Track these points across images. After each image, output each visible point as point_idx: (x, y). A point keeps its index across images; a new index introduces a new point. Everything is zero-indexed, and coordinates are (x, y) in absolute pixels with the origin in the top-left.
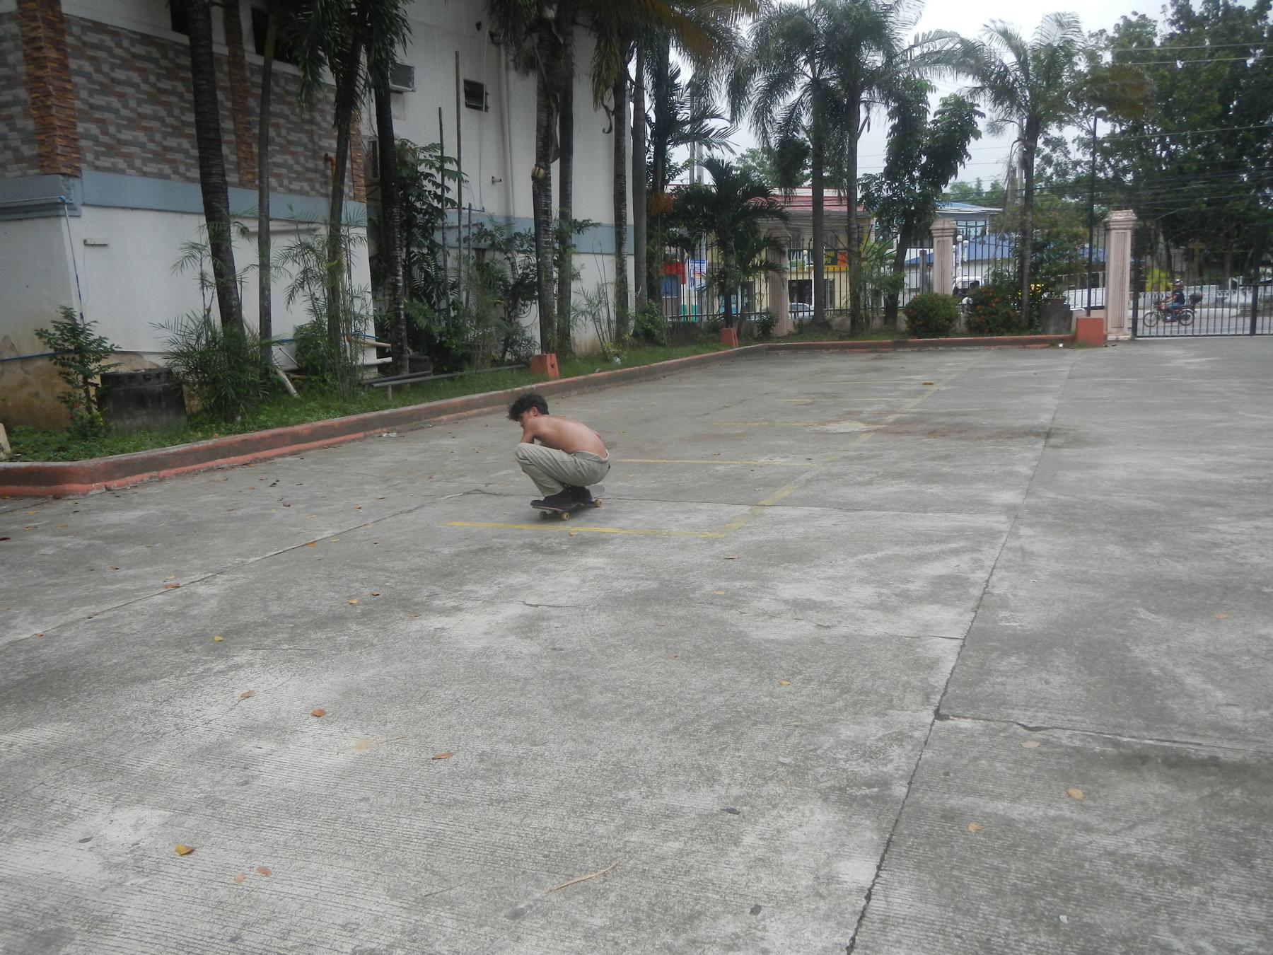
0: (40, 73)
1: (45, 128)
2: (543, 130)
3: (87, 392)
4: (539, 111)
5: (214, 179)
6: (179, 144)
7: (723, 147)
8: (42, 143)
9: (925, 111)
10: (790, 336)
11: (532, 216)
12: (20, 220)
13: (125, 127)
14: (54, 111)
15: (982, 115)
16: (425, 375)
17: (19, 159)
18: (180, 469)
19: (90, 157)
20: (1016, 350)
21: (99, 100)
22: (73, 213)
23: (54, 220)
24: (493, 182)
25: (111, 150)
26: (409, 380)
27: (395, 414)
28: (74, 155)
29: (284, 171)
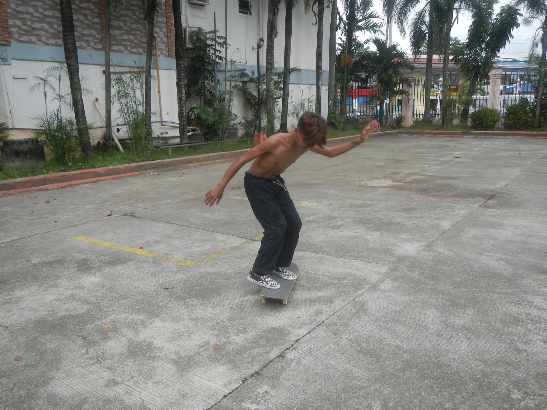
2: (270, 23)
4: (269, 13)
5: (69, 46)
6: (42, 27)
7: (379, 32)
9: (491, 14)
10: (412, 126)
11: (283, 67)
13: (36, 22)
15: (521, 15)
16: (197, 142)
18: (22, 190)
19: (16, 36)
20: (528, 139)
22: (4, 63)
24: (253, 49)
25: (28, 33)
26: (186, 145)
27: (161, 163)
28: (6, 35)
29: (128, 43)
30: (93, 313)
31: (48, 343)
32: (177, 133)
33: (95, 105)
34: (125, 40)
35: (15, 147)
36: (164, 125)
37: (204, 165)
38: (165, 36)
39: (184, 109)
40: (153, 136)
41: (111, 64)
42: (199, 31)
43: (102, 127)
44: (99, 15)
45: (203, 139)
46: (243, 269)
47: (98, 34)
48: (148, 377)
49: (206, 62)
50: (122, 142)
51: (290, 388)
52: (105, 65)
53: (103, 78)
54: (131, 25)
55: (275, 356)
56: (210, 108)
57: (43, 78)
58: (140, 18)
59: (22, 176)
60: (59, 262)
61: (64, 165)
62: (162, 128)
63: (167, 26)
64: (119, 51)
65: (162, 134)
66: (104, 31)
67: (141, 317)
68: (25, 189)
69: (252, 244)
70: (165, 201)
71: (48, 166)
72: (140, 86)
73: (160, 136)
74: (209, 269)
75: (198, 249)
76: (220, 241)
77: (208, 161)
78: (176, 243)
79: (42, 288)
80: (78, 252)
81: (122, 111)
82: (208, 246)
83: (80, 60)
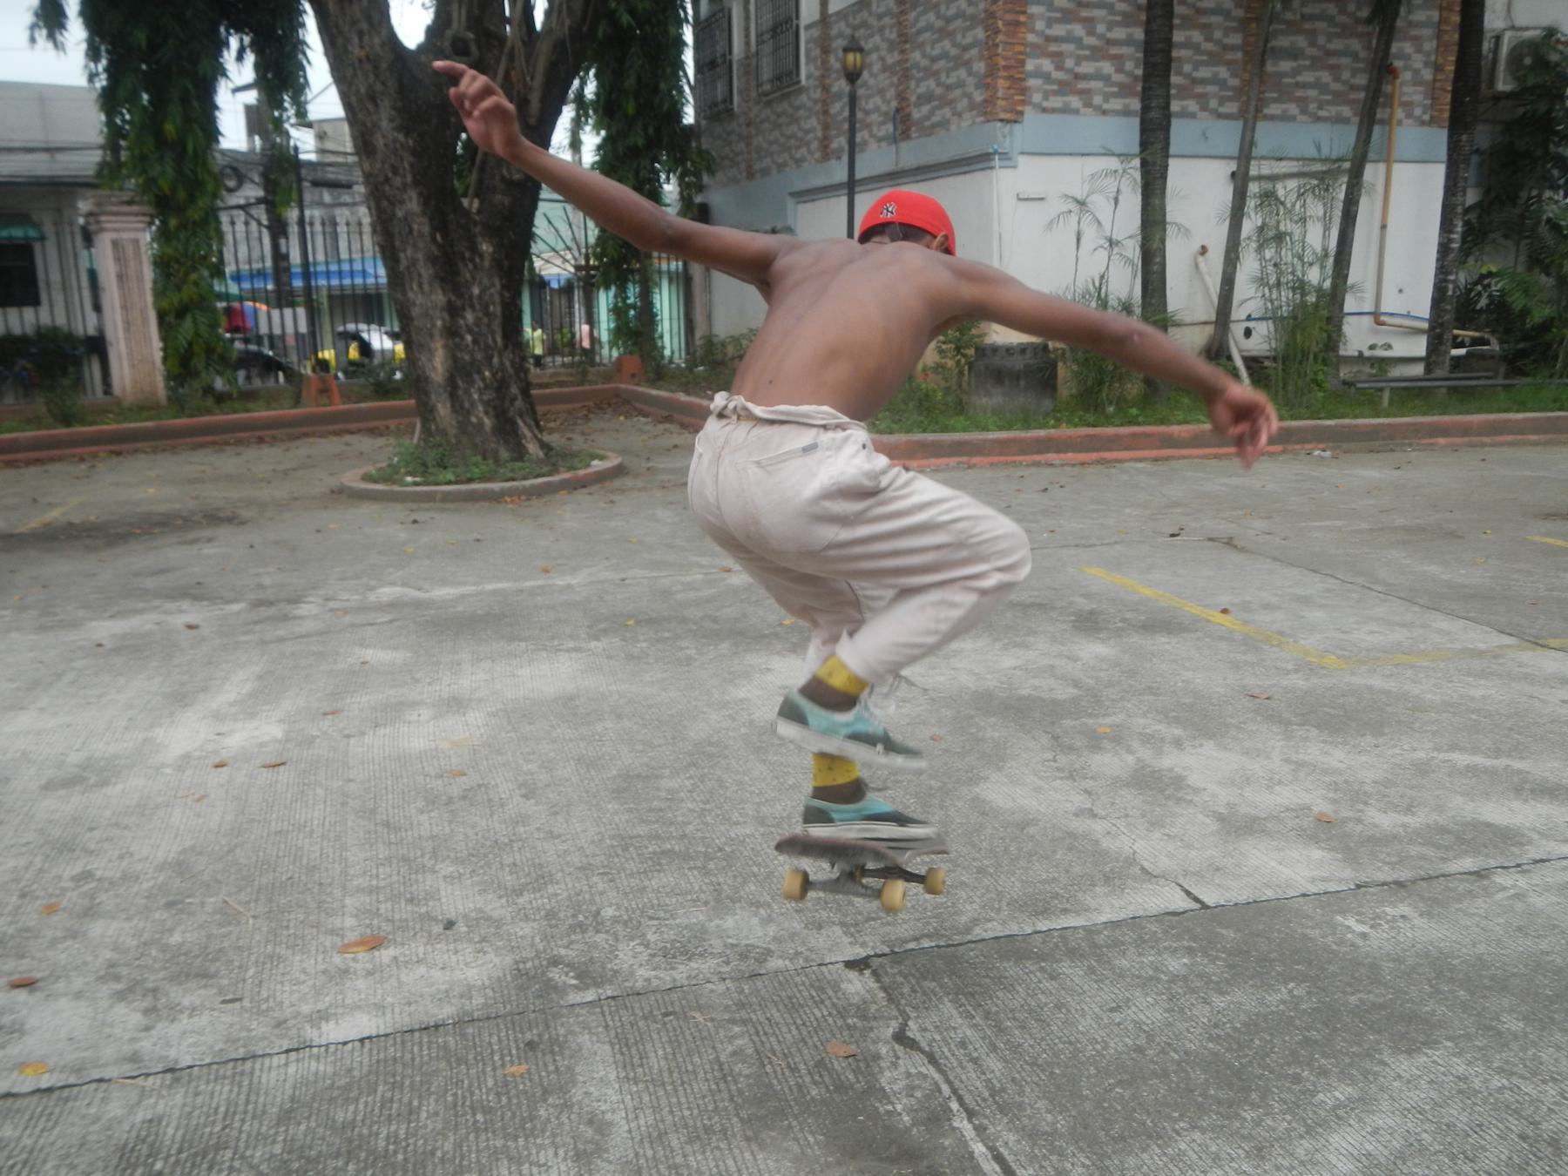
0: (994, 8)
1: (992, 71)
3: (959, 362)
5: (1153, 114)
8: (988, 86)
12: (965, 173)
13: (1086, 58)
14: (1000, 50)
16: (1478, 378)
17: (972, 107)
18: (996, 459)
19: (1037, 98)
21: (1059, 30)
23: (988, 172)
25: (1064, 88)
27: (1349, 426)
28: (1016, 98)
29: (1312, 93)
30: (1083, 704)
31: (990, 729)
32: (1419, 347)
33: (1196, 265)
34: (1304, 86)
35: (997, 361)
36: (1383, 324)
37: (1484, 445)
38: (1426, 64)
39: (1452, 277)
40: (1342, 352)
41: (1253, 154)
42: (1545, 37)
43: (1205, 323)
44: (1244, 24)
45: (1503, 369)
46: (1473, 698)
47: (1233, 75)
48: (1156, 824)
49: (1557, 133)
50: (1252, 364)
51: (1467, 927)
52: (1239, 158)
53: (1227, 193)
54: (1329, 41)
55: (1461, 870)
56: (1548, 275)
57: (1079, 198)
58: (1358, 21)
59: (1001, 428)
60: (1042, 607)
61: (1096, 408)
62: (1375, 332)
63: (1439, 35)
64: (1285, 118)
65: (1372, 347)
66: (1249, 67)
67: (1178, 732)
68: (1003, 459)
69: (1530, 653)
70: (1327, 523)
71: (1060, 411)
72: (1321, 213)
73: (1367, 353)
74: (1377, 682)
75: (1367, 636)
76: (1440, 632)
77: (1501, 434)
78: (1317, 615)
79: (998, 645)
80: (1083, 595)
81: (1261, 281)
82: (1400, 635)
83: (1172, 150)
